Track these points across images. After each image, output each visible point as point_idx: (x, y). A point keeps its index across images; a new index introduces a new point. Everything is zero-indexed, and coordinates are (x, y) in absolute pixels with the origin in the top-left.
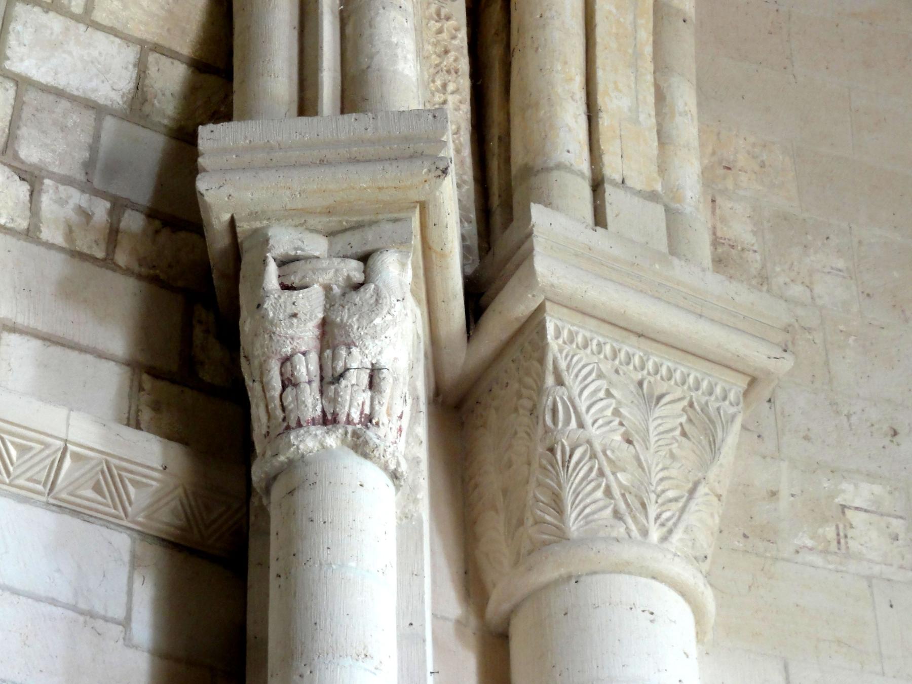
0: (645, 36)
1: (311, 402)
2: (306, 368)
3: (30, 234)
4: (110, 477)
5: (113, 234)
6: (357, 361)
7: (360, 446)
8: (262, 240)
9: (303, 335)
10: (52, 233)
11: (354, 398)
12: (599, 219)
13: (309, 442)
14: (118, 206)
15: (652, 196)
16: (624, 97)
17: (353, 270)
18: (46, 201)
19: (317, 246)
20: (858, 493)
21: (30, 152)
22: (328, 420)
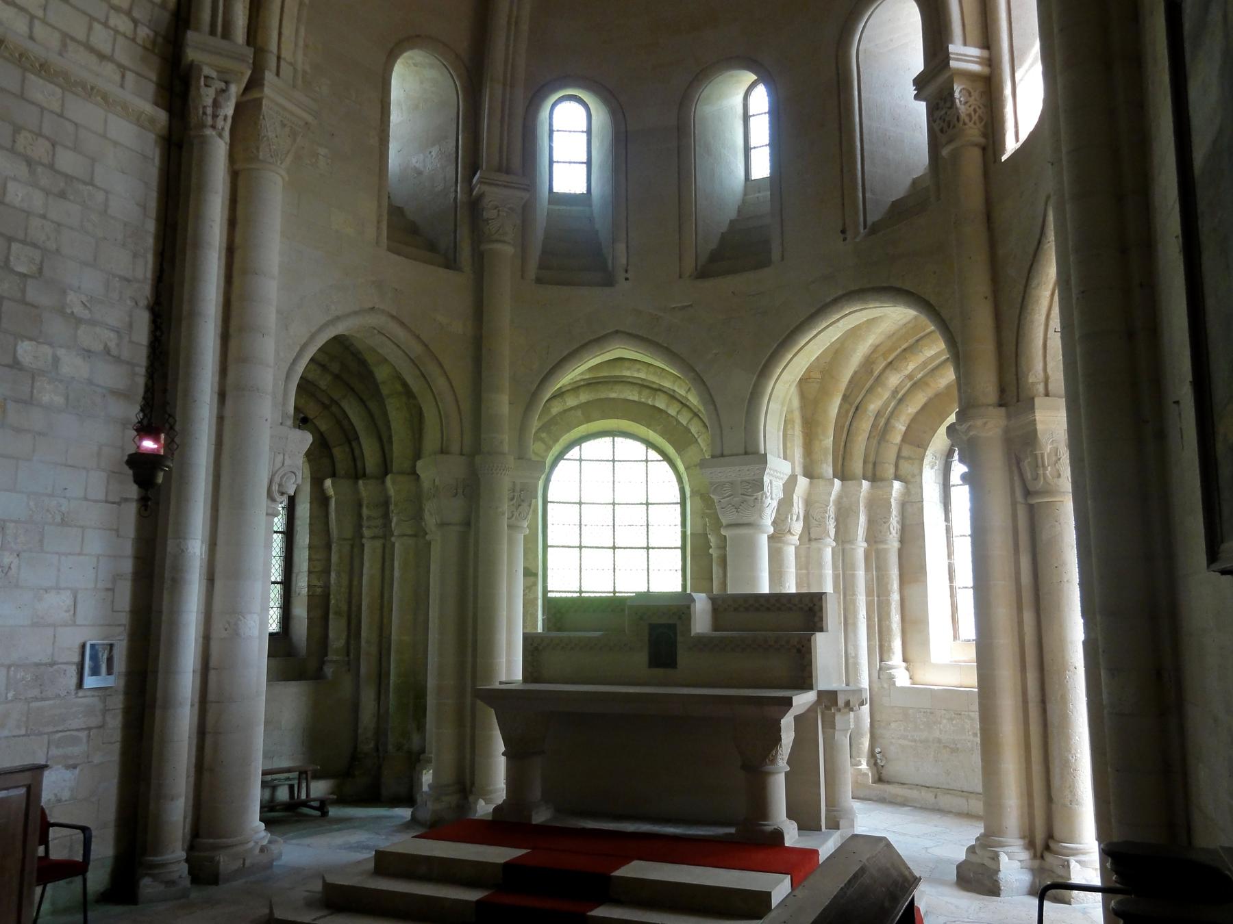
0: (296, 10)
1: (209, 121)
2: (209, 111)
3: (134, 40)
4: (152, 121)
5: (154, 43)
6: (222, 113)
7: (220, 136)
8: (200, 70)
9: (209, 101)
10: (139, 41)
11: (220, 123)
12: (278, 74)
13: (209, 132)
14: (156, 34)
15: (291, 64)
16: (288, 31)
17: (223, 85)
18: (139, 29)
19: (214, 74)
20: (322, 151)
21: (135, 14)
22: (213, 127)
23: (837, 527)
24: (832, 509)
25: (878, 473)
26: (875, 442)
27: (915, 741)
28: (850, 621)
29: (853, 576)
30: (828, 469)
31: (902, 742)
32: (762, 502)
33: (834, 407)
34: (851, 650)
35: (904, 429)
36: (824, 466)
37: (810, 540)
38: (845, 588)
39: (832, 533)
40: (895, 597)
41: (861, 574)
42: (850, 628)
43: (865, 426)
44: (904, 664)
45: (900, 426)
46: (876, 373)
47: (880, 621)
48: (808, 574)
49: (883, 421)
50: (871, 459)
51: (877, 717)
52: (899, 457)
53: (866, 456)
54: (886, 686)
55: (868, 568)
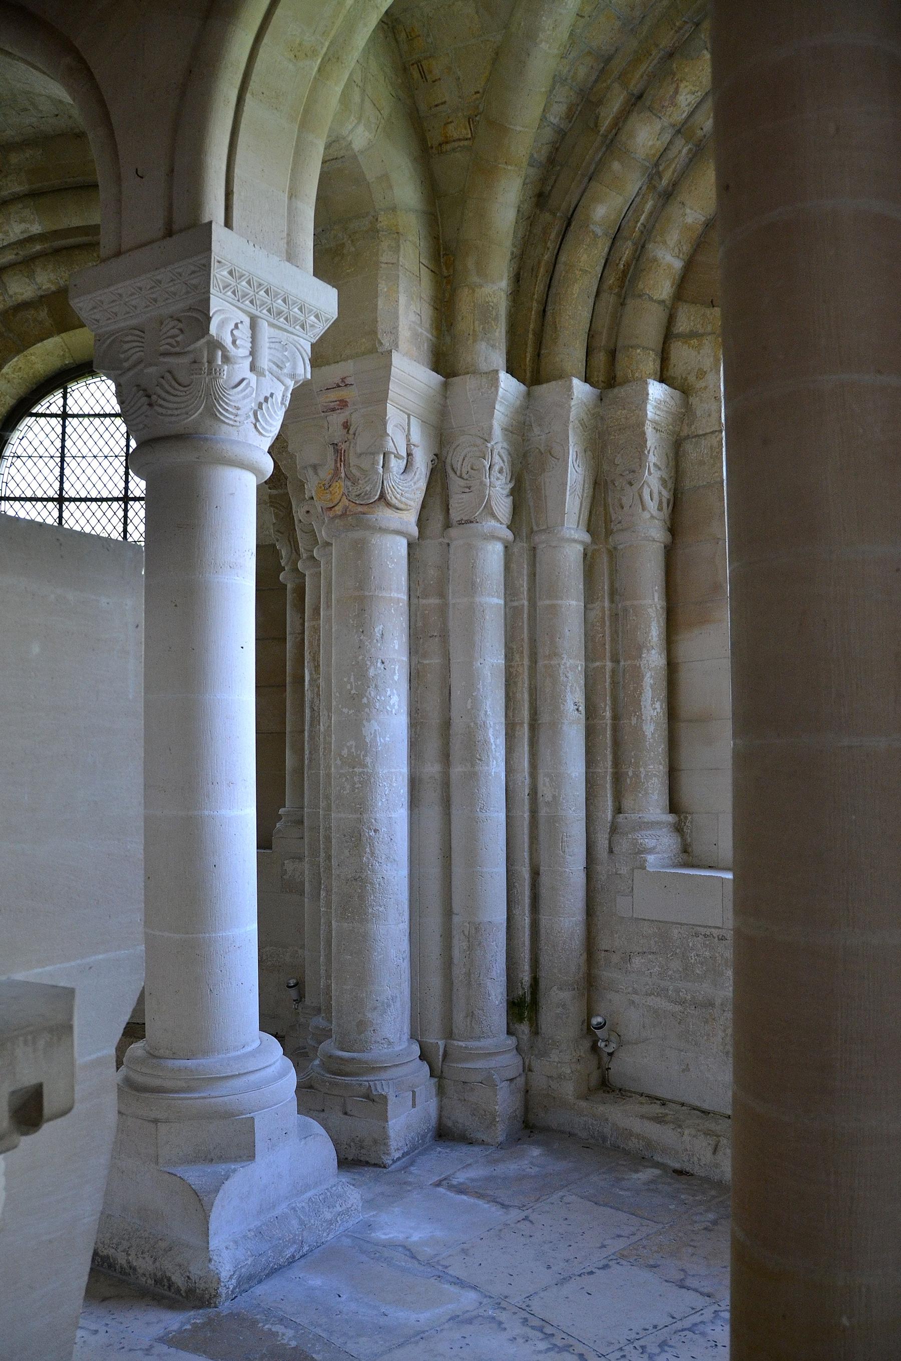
23: (517, 493)
24: (499, 442)
25: (619, 374)
26: (612, 299)
27: (682, 1002)
28: (544, 718)
29: (553, 610)
30: (492, 354)
31: (652, 1001)
32: (213, 372)
33: (505, 205)
34: (545, 790)
35: (678, 264)
36: (482, 346)
37: (447, 525)
38: (533, 641)
39: (502, 505)
40: (653, 659)
41: (572, 604)
42: (543, 739)
43: (586, 261)
44: (670, 818)
45: (668, 257)
46: (605, 124)
47: (616, 717)
48: (443, 610)
49: (626, 251)
50: (602, 340)
51: (604, 942)
52: (668, 336)
53: (591, 335)
54: (624, 870)
55: (590, 596)
